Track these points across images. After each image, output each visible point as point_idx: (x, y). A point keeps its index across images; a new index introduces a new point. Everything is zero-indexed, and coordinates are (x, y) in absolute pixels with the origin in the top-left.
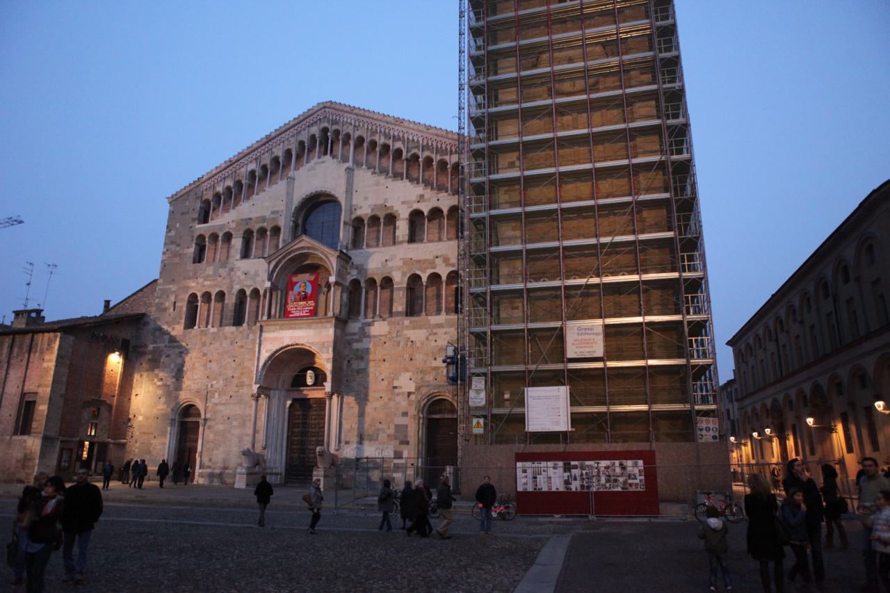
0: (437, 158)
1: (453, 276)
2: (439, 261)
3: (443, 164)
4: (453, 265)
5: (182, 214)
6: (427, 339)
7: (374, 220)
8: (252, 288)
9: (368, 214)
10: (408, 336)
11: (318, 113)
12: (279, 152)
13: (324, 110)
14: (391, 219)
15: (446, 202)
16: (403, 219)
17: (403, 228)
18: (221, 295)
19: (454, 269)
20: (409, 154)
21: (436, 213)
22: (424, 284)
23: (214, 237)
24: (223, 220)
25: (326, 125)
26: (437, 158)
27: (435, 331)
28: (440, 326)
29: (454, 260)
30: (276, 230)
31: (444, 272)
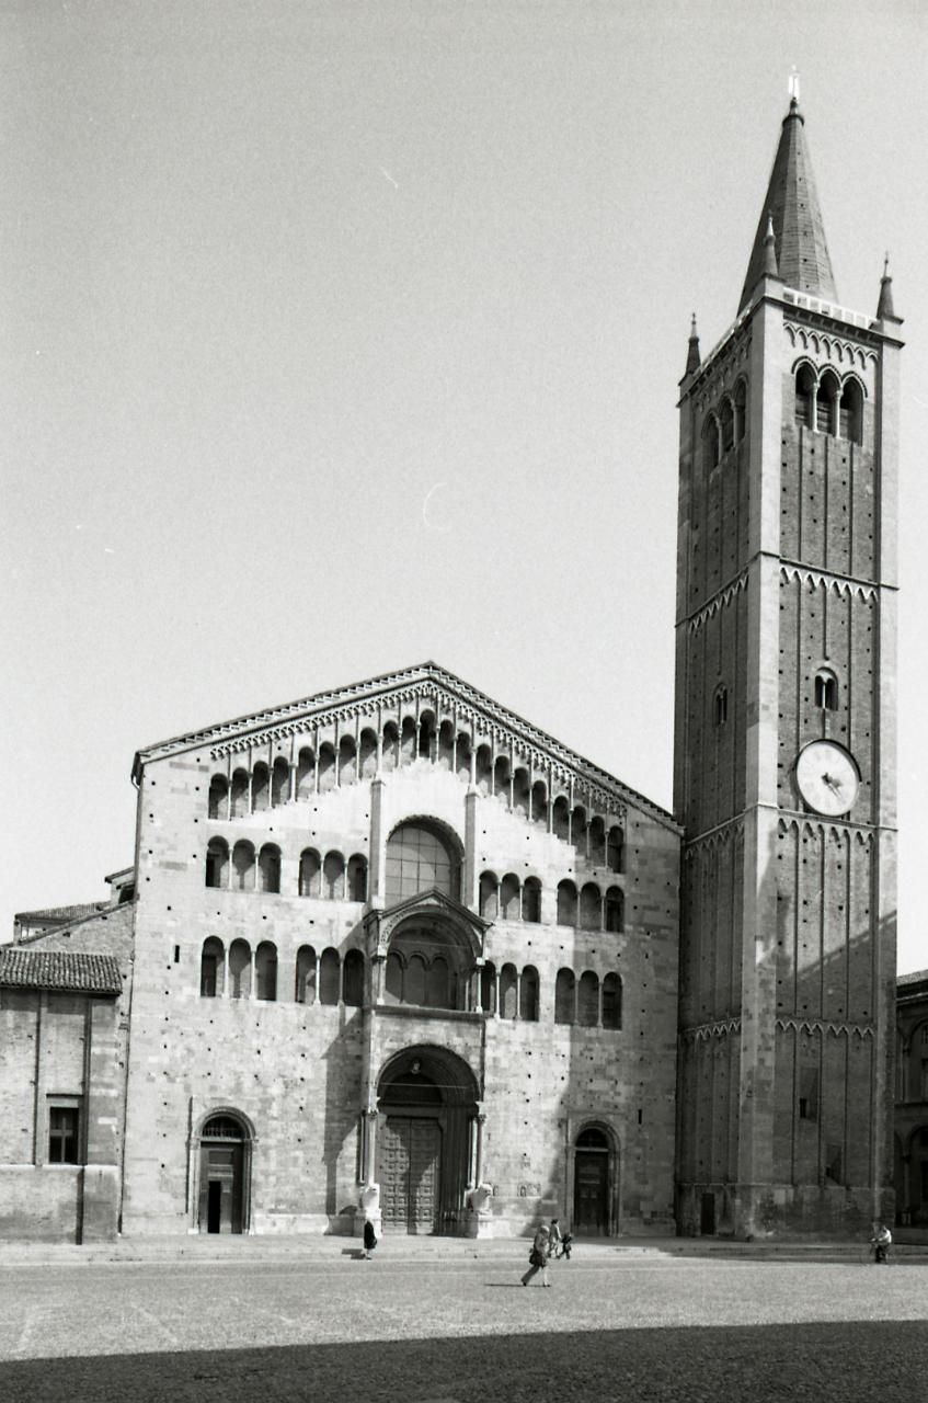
0: (591, 814)
1: (613, 978)
2: (596, 957)
3: (598, 823)
4: (611, 965)
5: (173, 790)
6: (581, 1054)
7: (510, 879)
8: (324, 948)
9: (500, 871)
10: (559, 1047)
11: (417, 685)
12: (350, 728)
13: (427, 682)
14: (534, 885)
15: (606, 879)
16: (549, 889)
17: (549, 902)
18: (267, 948)
19: (613, 970)
20: (554, 797)
21: (591, 888)
22: (577, 984)
23: (244, 846)
24: (253, 823)
25: (432, 709)
26: (591, 814)
27: (590, 1046)
28: (599, 1040)
29: (613, 960)
30: (360, 865)
31: (601, 972)
